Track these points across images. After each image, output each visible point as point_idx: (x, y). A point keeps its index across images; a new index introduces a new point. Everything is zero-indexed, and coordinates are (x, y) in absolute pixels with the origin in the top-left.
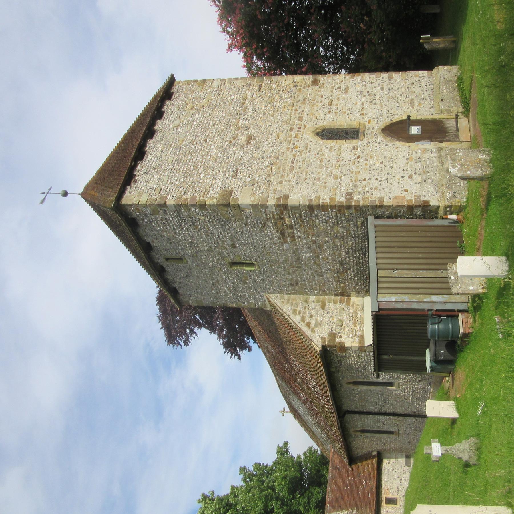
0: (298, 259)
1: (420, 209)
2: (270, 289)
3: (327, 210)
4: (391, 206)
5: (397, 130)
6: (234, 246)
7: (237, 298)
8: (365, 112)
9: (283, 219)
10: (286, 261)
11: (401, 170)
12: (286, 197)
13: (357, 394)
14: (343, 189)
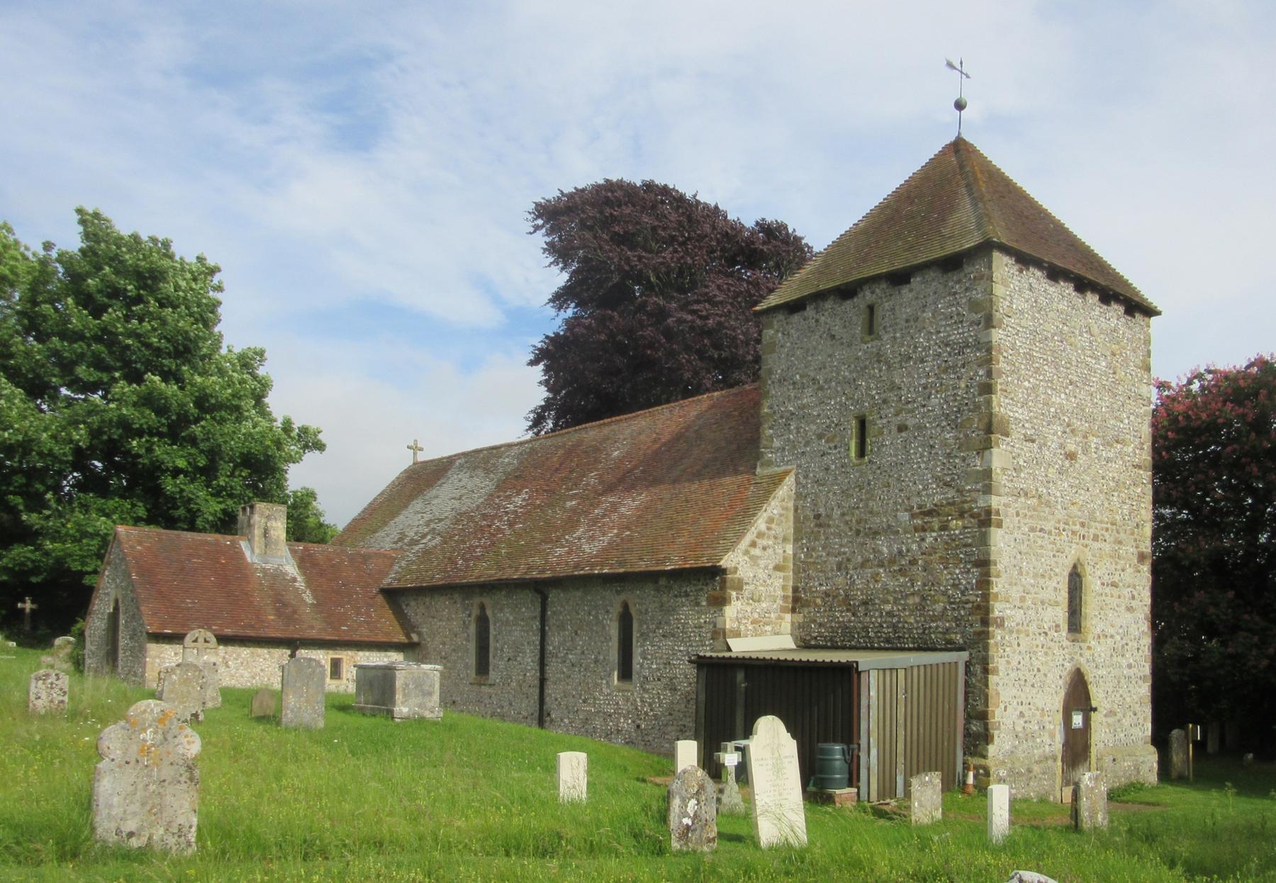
0: (875, 534)
1: (981, 730)
2: (806, 477)
3: (978, 589)
4: (987, 686)
5: (1078, 694)
6: (902, 428)
7: (782, 417)
8: (1102, 640)
9: (961, 515)
10: (871, 512)
11: (1030, 700)
12: (999, 525)
13: (596, 617)
14: (1008, 612)
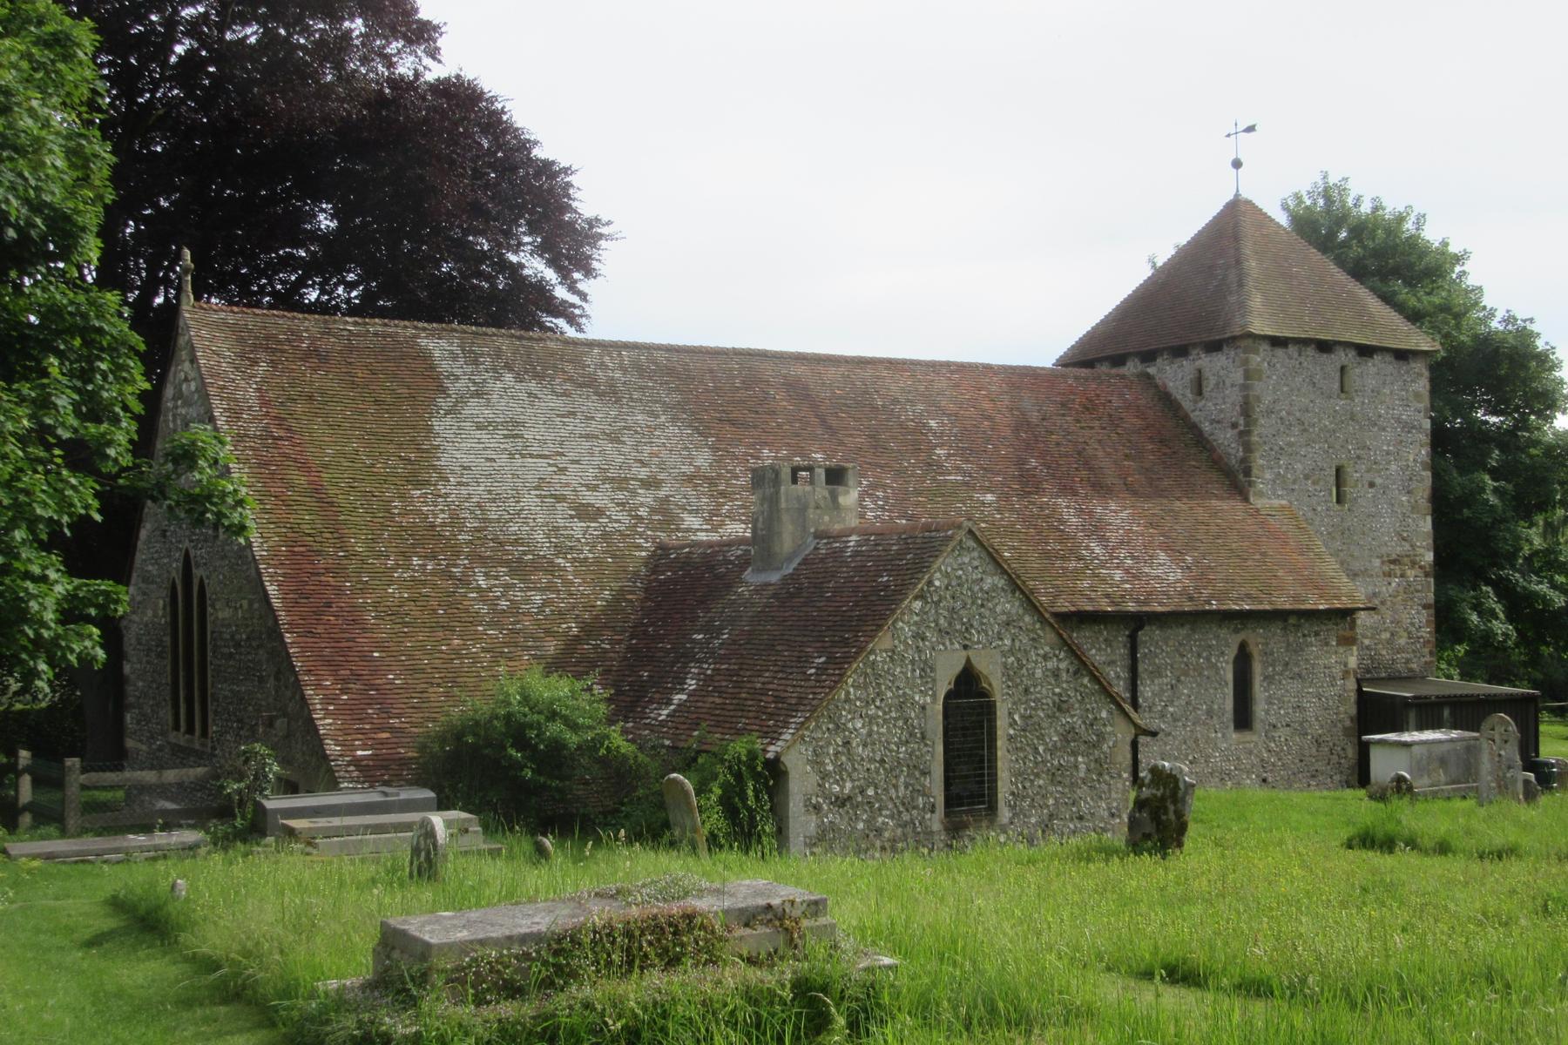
6: (1372, 485)
9: (1412, 567)
13: (1208, 659)
